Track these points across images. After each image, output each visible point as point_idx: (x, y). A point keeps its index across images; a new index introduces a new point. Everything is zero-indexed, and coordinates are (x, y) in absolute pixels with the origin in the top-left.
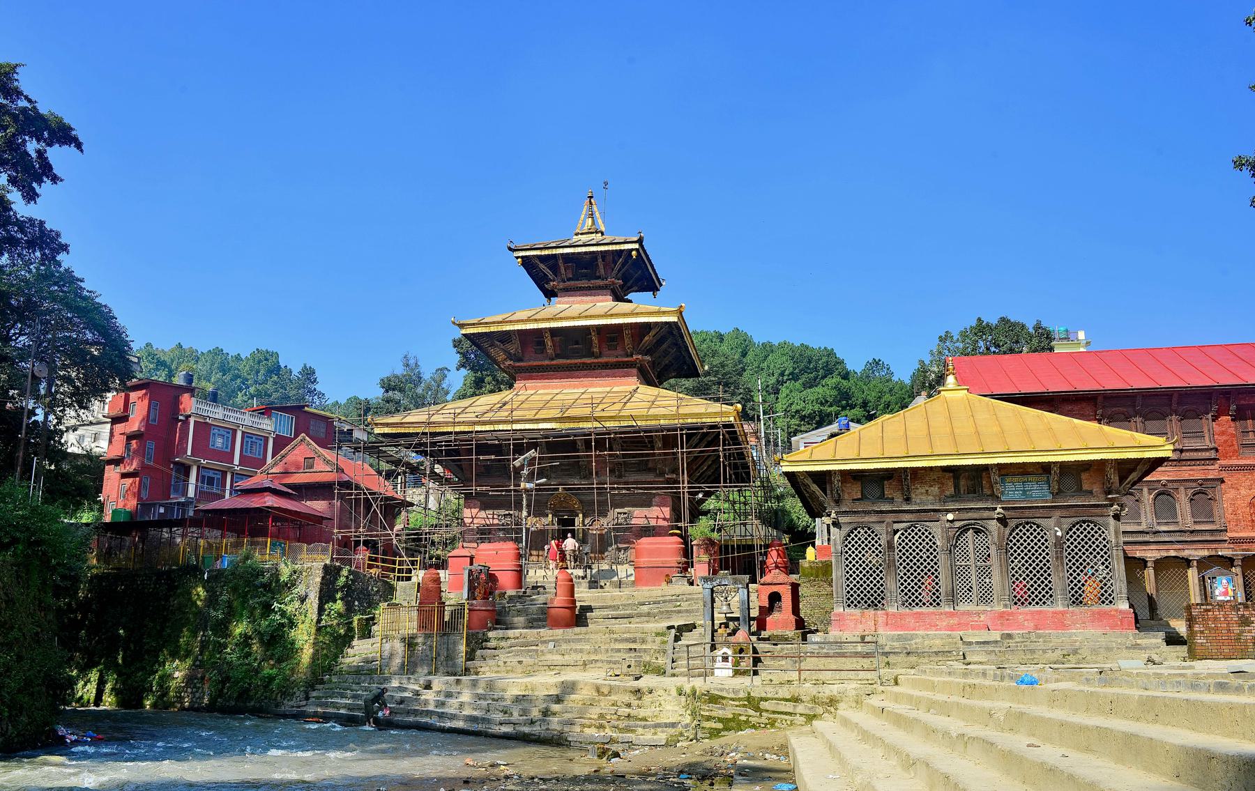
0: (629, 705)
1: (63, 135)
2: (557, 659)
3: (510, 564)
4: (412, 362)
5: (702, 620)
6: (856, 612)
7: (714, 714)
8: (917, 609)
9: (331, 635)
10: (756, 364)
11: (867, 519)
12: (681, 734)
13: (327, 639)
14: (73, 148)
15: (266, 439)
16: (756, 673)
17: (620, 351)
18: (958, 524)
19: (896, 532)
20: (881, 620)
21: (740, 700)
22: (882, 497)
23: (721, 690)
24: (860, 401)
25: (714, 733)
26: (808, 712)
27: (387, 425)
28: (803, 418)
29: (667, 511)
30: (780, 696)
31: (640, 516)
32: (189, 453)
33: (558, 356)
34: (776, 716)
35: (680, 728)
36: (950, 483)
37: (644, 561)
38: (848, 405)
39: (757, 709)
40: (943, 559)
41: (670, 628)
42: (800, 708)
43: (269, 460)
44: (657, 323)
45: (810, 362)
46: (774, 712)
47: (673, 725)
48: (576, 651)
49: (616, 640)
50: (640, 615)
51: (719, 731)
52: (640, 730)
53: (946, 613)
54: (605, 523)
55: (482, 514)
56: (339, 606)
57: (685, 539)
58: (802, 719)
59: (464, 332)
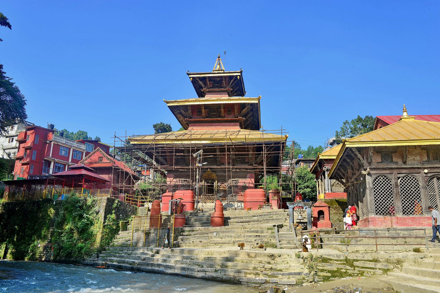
0: (269, 263)
2: (218, 240)
3: (189, 199)
5: (287, 223)
7: (325, 268)
8: (411, 216)
9: (110, 229)
11: (384, 172)
12: (304, 279)
13: (108, 231)
15: (83, 153)
16: (321, 247)
17: (232, 115)
18: (429, 175)
19: (399, 178)
20: (394, 220)
21: (341, 260)
22: (392, 161)
23: (330, 255)
25: (326, 279)
26: (384, 268)
27: (136, 140)
29: (253, 180)
30: (366, 258)
31: (241, 182)
32: (51, 156)
33: (207, 117)
34: (364, 269)
35: (303, 276)
36: (425, 155)
37: (248, 199)
39: (352, 266)
40: (422, 191)
41: (274, 226)
42: (379, 265)
43: (84, 158)
44: (249, 104)
46: (362, 268)
47: (299, 274)
48: (228, 236)
49: (248, 231)
50: (254, 221)
51: (329, 277)
52: (280, 276)
53: (427, 218)
54: (225, 186)
55: (175, 180)
56: (113, 216)
58: (381, 271)
59: (168, 105)
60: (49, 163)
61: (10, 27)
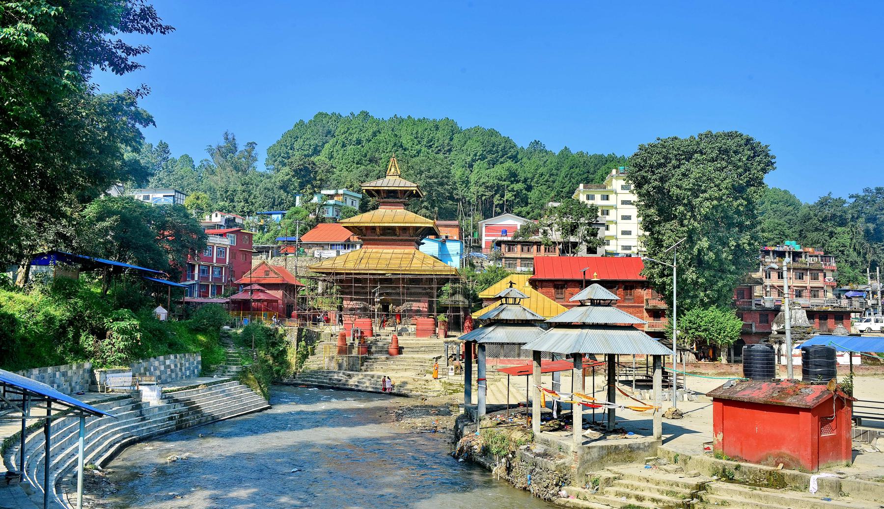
1: (148, 121)
2: (395, 367)
3: (369, 327)
4: (230, 137)
10: (459, 147)
14: (151, 125)
25: (451, 394)
28: (487, 187)
31: (415, 306)
33: (381, 235)
45: (493, 146)
56: (303, 343)
57: (435, 319)
60: (193, 266)
61: (154, 124)
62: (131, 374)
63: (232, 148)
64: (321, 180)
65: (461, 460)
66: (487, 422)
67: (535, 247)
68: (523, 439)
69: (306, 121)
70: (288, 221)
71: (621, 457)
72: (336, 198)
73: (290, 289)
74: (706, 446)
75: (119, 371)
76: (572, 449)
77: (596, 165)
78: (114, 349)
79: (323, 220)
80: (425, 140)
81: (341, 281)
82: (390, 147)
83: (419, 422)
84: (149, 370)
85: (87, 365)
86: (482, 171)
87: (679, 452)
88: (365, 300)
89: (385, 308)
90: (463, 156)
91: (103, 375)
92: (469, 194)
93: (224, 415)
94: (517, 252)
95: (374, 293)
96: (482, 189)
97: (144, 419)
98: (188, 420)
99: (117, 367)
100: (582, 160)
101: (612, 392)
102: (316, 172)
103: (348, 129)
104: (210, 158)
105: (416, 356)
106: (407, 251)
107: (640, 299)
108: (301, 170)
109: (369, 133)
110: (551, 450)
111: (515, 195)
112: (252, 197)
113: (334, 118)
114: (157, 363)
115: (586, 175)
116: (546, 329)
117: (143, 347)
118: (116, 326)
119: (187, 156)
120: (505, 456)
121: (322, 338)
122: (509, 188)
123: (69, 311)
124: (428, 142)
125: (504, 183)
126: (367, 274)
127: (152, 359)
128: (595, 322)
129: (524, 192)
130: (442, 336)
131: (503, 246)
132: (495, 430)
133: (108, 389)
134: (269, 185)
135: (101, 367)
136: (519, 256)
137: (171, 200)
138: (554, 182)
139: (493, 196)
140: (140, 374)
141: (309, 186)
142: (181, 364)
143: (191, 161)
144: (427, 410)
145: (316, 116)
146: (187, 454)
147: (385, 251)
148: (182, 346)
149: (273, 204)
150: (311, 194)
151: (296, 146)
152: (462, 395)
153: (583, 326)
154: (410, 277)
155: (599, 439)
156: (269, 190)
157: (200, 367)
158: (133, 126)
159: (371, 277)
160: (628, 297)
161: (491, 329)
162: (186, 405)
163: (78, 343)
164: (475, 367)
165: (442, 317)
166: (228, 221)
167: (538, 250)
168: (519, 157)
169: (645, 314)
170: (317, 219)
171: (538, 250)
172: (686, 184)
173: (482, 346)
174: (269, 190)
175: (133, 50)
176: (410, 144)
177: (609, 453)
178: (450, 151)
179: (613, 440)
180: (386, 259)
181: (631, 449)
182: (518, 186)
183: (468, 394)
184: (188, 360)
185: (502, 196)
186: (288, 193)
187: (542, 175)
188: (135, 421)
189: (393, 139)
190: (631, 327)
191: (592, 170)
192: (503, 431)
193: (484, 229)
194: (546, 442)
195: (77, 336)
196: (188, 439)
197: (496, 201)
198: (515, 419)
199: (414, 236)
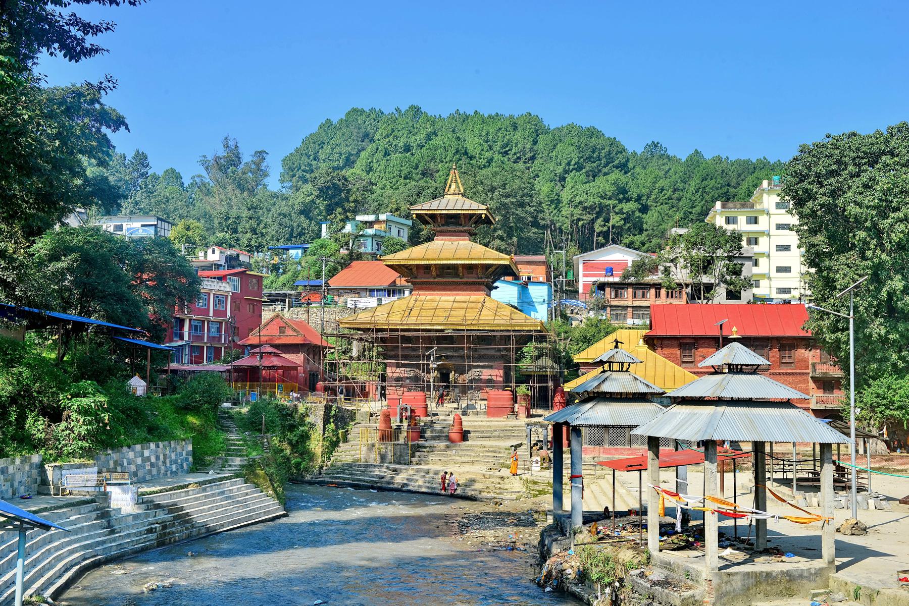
1: (118, 123)
2: (457, 458)
3: (422, 404)
4: (232, 144)
6: (591, 447)
10: (546, 153)
13: (327, 444)
14: (123, 128)
17: (474, 275)
24: (635, 196)
25: (535, 496)
28: (585, 208)
29: (501, 372)
31: (486, 374)
33: (438, 276)
38: (624, 198)
45: (594, 151)
50: (494, 437)
55: (398, 370)
56: (332, 426)
57: (514, 392)
60: (182, 322)
61: (127, 128)
62: (96, 469)
63: (234, 159)
64: (354, 201)
65: (548, 589)
66: (584, 536)
67: (653, 291)
68: (635, 561)
69: (335, 120)
70: (311, 259)
71: (775, 588)
72: (376, 226)
73: (314, 351)
74: (902, 576)
75: (79, 466)
76: (704, 576)
77: (740, 175)
78: (72, 436)
79: (359, 257)
80: (499, 144)
81: (384, 340)
82: (450, 154)
83: (491, 535)
84: (121, 465)
85: (36, 458)
86: (579, 186)
87: (862, 583)
88: (417, 366)
89: (444, 377)
90: (551, 166)
91: (58, 472)
92: (561, 219)
93: (222, 526)
94: (628, 298)
95: (429, 356)
96: (578, 211)
97: (113, 532)
98: (173, 533)
99: (77, 461)
100: (719, 168)
101: (761, 495)
102: (349, 191)
103: (393, 131)
104: (204, 173)
105: (486, 443)
106: (473, 298)
107: (804, 364)
108: (328, 188)
109: (422, 136)
110: (675, 577)
111: (625, 219)
112: (262, 225)
113: (372, 116)
114: (131, 455)
115: (725, 189)
116: (666, 406)
117: (113, 433)
118: (76, 403)
119: (173, 171)
120: (610, 584)
121: (358, 418)
122: (617, 209)
123: (11, 384)
124: (503, 147)
125: (610, 202)
126: (418, 330)
127: (125, 449)
128: (735, 396)
129: (637, 214)
130: (523, 415)
131: (608, 290)
132: (596, 547)
133: (63, 490)
134: (285, 210)
135: (55, 460)
136: (630, 304)
137: (152, 231)
138: (679, 199)
139: (593, 221)
140: (109, 470)
141: (339, 210)
142: (165, 455)
143: (179, 177)
144: (502, 518)
145: (348, 113)
146: (171, 580)
147: (444, 298)
148: (166, 431)
149: (291, 235)
150: (342, 220)
151: (322, 156)
152: (550, 498)
153: (719, 402)
154: (479, 334)
155: (744, 562)
156: (285, 216)
157: (191, 459)
158: (98, 130)
159: (425, 334)
160: (786, 360)
161: (589, 405)
162: (170, 511)
163: (23, 428)
164: (567, 458)
165: (522, 389)
166: (229, 259)
167: (658, 295)
168: (630, 165)
169: (812, 384)
170: (351, 255)
171: (658, 295)
172: (869, 200)
173: (576, 430)
174: (285, 216)
175: (92, 28)
176: (478, 150)
177: (758, 583)
178: (533, 158)
179: (763, 565)
180: (445, 310)
181: (791, 577)
182: (628, 207)
183: (558, 496)
184: (175, 450)
185: (607, 220)
186: (311, 220)
187: (662, 190)
188: (100, 535)
189: (455, 144)
190: (787, 404)
191: (733, 182)
192: (607, 549)
193: (581, 267)
194: (667, 566)
195: (22, 418)
196: (173, 559)
197: (598, 228)
198: (624, 533)
199: (482, 278)
